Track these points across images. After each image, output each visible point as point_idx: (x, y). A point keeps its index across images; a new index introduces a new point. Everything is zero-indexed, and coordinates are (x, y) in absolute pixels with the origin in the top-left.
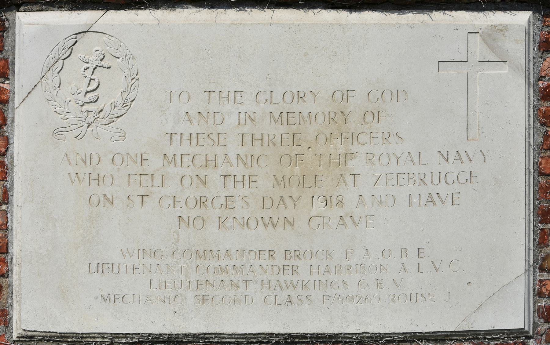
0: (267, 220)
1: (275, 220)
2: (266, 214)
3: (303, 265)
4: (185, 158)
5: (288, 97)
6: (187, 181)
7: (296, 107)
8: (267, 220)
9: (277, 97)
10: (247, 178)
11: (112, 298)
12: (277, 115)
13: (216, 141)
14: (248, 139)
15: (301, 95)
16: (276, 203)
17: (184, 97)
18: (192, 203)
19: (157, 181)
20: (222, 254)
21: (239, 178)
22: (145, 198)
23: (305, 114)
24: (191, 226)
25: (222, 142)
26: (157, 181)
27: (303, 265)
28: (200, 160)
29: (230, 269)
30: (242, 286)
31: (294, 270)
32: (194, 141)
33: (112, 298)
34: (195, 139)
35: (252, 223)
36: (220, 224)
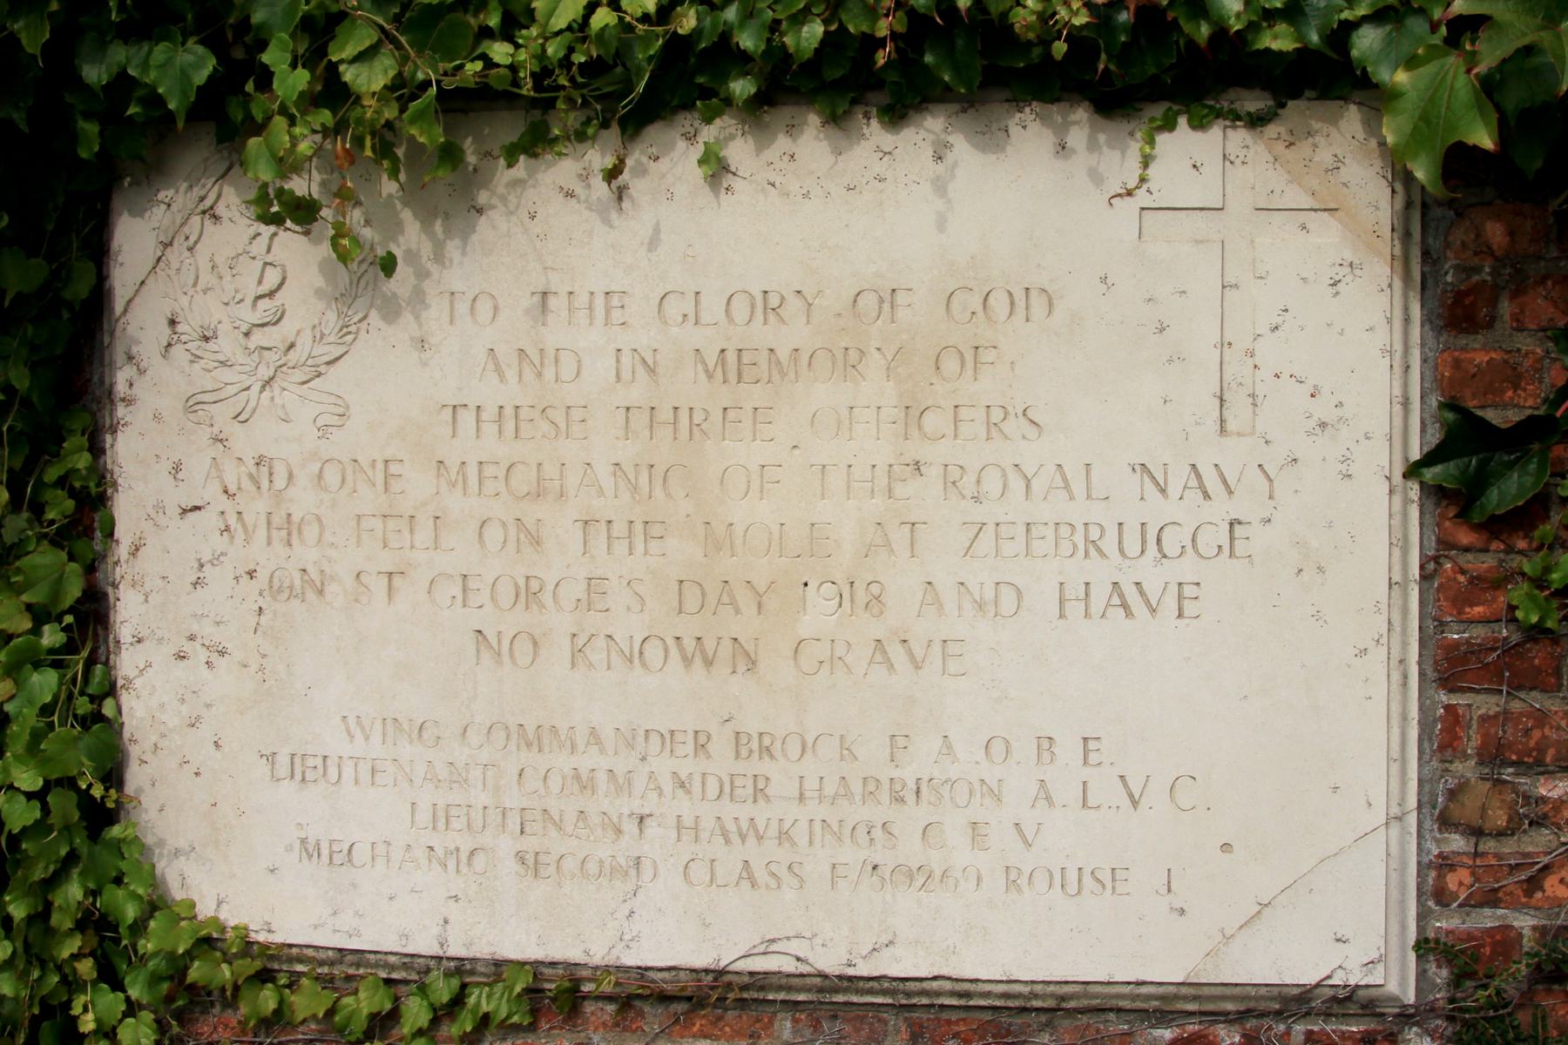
0: (690, 644)
1: (709, 645)
2: (688, 628)
3: (781, 775)
4: (489, 471)
5: (740, 309)
6: (494, 534)
7: (762, 334)
8: (690, 644)
9: (713, 308)
10: (639, 527)
11: (325, 852)
12: (712, 358)
13: (563, 426)
14: (640, 420)
15: (774, 301)
16: (712, 599)
17: (484, 308)
18: (506, 593)
19: (424, 535)
20: (581, 737)
21: (619, 529)
22: (397, 580)
23: (783, 354)
24: (506, 658)
25: (576, 429)
26: (424, 535)
27: (781, 775)
28: (523, 480)
29: (602, 777)
30: (630, 827)
31: (759, 793)
32: (510, 426)
33: (325, 852)
34: (511, 419)
35: (654, 652)
36: (577, 654)
